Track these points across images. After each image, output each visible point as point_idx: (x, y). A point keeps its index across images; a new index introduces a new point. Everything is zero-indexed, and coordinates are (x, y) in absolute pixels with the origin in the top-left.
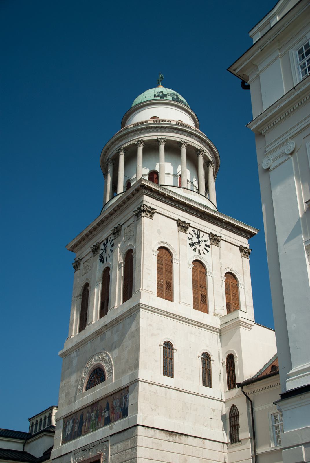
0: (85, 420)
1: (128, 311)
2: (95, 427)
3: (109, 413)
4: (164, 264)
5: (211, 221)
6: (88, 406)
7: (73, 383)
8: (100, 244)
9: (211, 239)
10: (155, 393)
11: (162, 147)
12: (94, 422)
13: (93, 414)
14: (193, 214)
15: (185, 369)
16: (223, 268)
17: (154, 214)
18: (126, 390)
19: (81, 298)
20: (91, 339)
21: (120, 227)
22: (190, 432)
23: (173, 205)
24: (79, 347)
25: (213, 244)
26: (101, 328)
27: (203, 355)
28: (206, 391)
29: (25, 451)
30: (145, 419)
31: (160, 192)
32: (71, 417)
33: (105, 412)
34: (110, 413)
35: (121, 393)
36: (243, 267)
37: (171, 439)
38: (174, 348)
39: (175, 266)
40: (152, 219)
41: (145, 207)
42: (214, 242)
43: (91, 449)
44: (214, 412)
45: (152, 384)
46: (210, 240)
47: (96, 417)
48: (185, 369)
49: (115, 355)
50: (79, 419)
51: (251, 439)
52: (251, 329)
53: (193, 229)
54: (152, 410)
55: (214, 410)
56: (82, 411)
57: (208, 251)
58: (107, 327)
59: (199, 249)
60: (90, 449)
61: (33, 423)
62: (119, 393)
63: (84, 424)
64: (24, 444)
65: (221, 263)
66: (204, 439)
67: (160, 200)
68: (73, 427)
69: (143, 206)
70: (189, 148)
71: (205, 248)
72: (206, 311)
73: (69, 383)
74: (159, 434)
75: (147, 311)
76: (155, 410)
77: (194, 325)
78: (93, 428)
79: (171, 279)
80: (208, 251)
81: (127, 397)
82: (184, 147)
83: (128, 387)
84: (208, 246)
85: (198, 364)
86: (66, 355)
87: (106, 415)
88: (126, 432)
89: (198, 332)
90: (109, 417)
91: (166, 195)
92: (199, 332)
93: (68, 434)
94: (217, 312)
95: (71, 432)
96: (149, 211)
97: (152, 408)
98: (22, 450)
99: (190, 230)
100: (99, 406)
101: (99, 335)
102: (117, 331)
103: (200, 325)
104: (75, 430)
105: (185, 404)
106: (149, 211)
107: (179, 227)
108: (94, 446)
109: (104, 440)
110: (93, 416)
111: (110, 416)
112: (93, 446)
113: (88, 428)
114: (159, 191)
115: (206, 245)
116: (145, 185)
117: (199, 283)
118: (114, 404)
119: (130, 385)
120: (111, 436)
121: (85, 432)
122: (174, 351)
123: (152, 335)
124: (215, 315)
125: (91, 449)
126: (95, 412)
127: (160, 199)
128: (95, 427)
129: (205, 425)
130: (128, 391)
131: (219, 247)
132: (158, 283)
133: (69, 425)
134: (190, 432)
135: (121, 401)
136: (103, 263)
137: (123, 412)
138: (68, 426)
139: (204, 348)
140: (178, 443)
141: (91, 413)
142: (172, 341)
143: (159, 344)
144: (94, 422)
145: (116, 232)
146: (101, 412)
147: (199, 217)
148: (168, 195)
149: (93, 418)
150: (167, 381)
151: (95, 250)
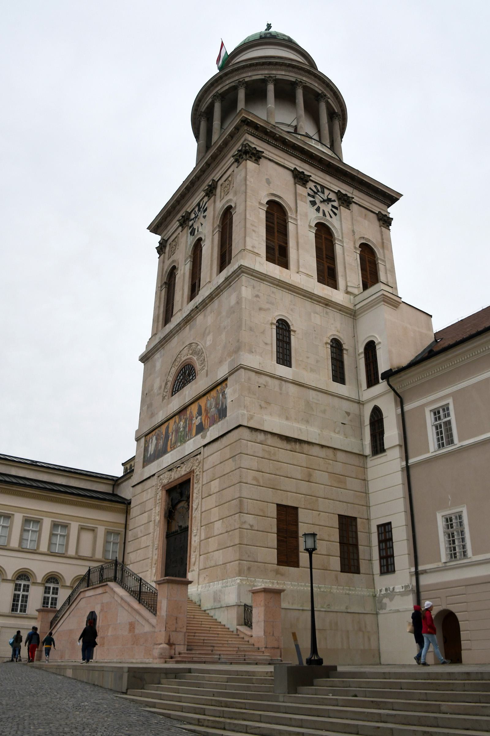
0: (171, 434)
1: (225, 279)
2: (184, 439)
3: (201, 419)
4: (276, 223)
5: (338, 177)
6: (174, 415)
7: (156, 391)
8: (190, 213)
9: (339, 199)
10: (265, 386)
11: (271, 88)
12: (182, 434)
13: (182, 423)
14: (315, 165)
15: (308, 358)
16: (357, 237)
17: (261, 158)
18: (224, 385)
19: (167, 287)
20: (177, 331)
21: (215, 183)
22: (316, 439)
23: (287, 150)
24: (163, 345)
25: (343, 206)
26: (190, 313)
27: (331, 341)
28: (337, 388)
29: (115, 493)
30: (251, 418)
31: (269, 131)
32: (154, 433)
33: (197, 418)
34: (203, 418)
35: (217, 390)
36: (382, 239)
37: (289, 447)
38: (292, 328)
39: (291, 227)
40: (259, 165)
41: (247, 148)
42: (343, 203)
43: (179, 467)
44: (348, 416)
45: (261, 374)
46: (339, 201)
47: (184, 428)
48: (308, 358)
49: (208, 343)
50: (164, 433)
51: (400, 446)
52: (396, 307)
53: (315, 184)
54: (261, 407)
55: (348, 414)
56: (166, 424)
57: (335, 214)
58: (198, 310)
59: (324, 209)
60: (177, 468)
61: (127, 468)
62: (215, 391)
63: (170, 438)
64: (114, 485)
65: (353, 232)
66: (335, 449)
67: (268, 143)
68: (157, 445)
69: (245, 147)
70: (307, 90)
71: (332, 210)
72: (335, 286)
73: (152, 392)
74: (270, 440)
75: (252, 278)
76: (266, 408)
77: (319, 302)
78: (181, 441)
79: (286, 242)
80: (335, 214)
81: (225, 392)
82: (300, 88)
83: (226, 379)
84: (336, 208)
85: (326, 353)
86: (148, 359)
88: (225, 438)
89: (325, 312)
90: (201, 424)
91: (277, 136)
92: (326, 312)
93: (152, 452)
94: (350, 289)
95: (155, 451)
96: (253, 154)
97: (260, 406)
98: (111, 492)
99: (311, 185)
100: (188, 412)
101: (187, 324)
102: (211, 312)
103: (327, 303)
105: (309, 402)
106: (253, 154)
107: (296, 179)
108: (182, 463)
109: (195, 453)
110: (181, 426)
112: (183, 461)
113: (175, 443)
114: (266, 129)
115: (333, 206)
116: (247, 119)
117: (324, 252)
118: (208, 405)
119: (230, 375)
120: (204, 446)
121: (171, 448)
122: (292, 333)
123: (260, 309)
124: (347, 293)
125: (179, 467)
126: (184, 421)
127: (269, 141)
128: (184, 439)
129: (336, 431)
130: (226, 385)
131: (350, 210)
132: (267, 246)
134: (316, 439)
135: (217, 398)
136: (194, 235)
137: (220, 414)
138: (150, 445)
139: (334, 333)
140: (299, 453)
141: (179, 422)
142: (289, 319)
143: (270, 322)
144: (183, 433)
146: (191, 420)
147: (322, 171)
148: (280, 136)
149: (181, 429)
150: (282, 370)
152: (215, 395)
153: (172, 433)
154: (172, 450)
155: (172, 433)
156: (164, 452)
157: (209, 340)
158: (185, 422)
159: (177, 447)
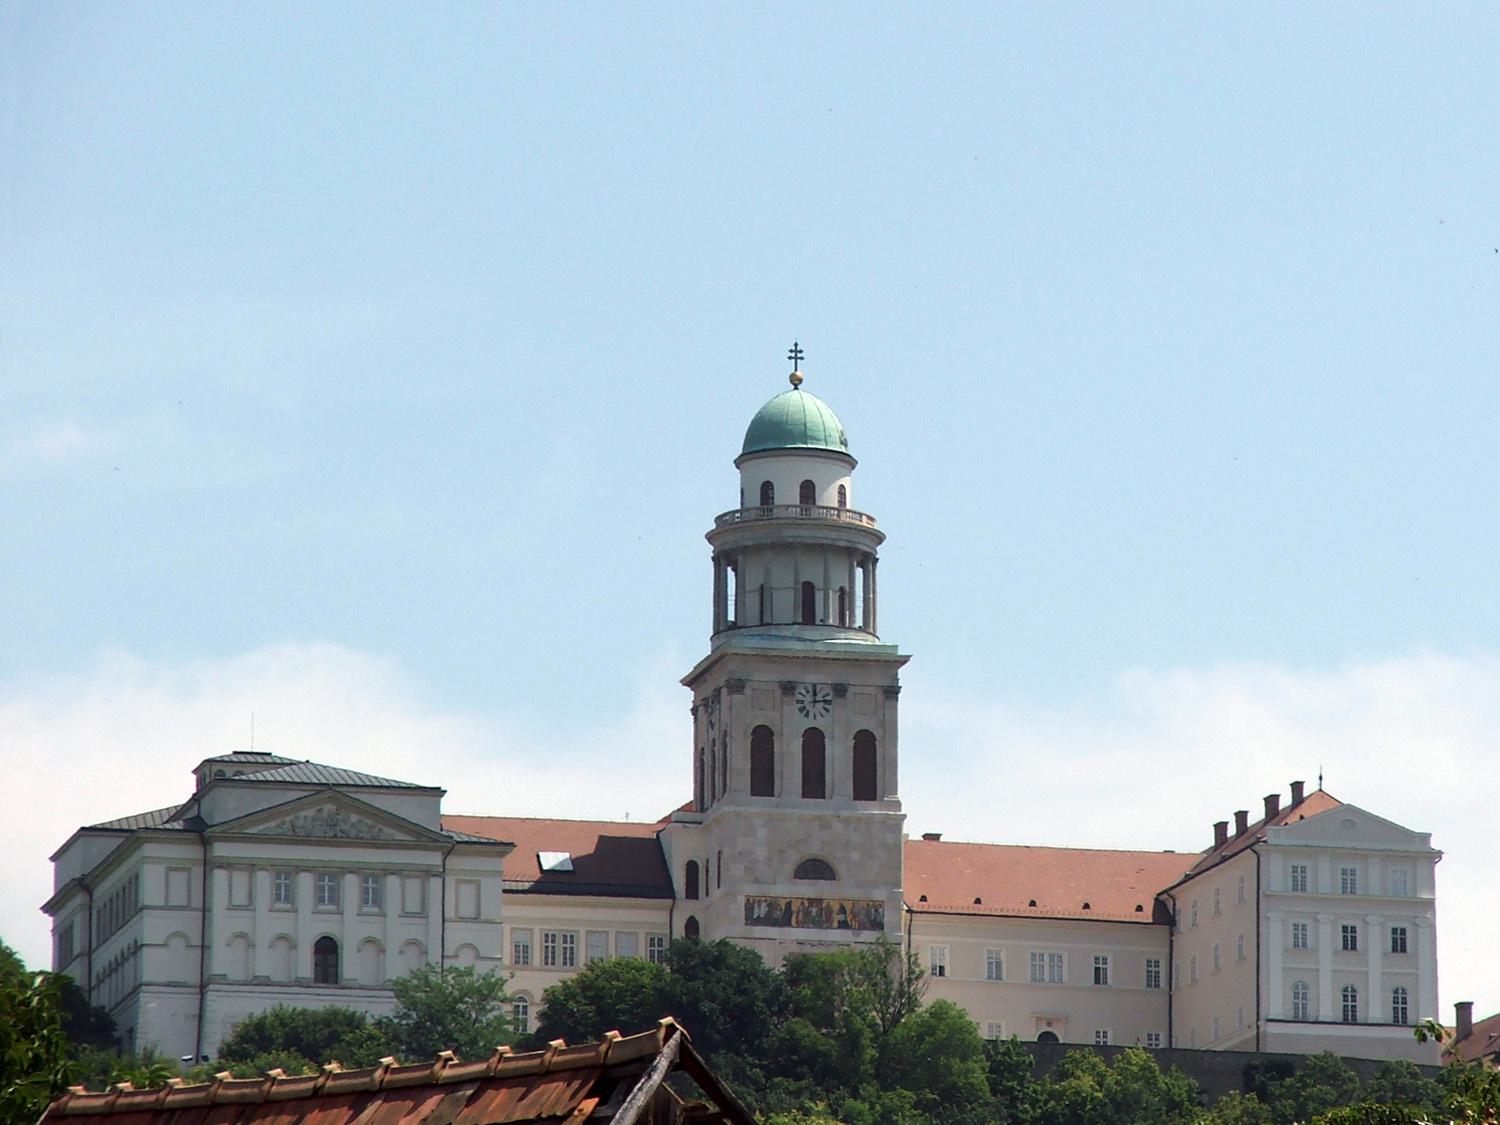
87: (842, 917)
104: (775, 916)
111: (849, 922)
112: (821, 943)
133: (759, 906)
145: (840, 690)
151: (788, 688)
152: (865, 906)
153: (798, 913)
154: (798, 927)
155: (798, 913)
156: (789, 924)
157: (855, 856)
158: (821, 910)
159: (808, 927)
